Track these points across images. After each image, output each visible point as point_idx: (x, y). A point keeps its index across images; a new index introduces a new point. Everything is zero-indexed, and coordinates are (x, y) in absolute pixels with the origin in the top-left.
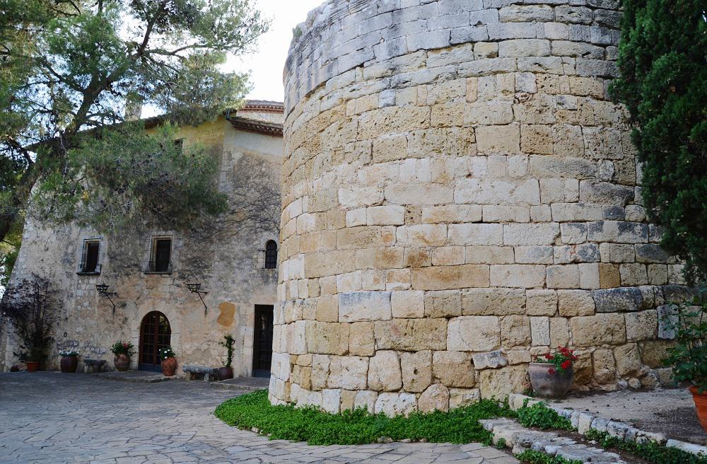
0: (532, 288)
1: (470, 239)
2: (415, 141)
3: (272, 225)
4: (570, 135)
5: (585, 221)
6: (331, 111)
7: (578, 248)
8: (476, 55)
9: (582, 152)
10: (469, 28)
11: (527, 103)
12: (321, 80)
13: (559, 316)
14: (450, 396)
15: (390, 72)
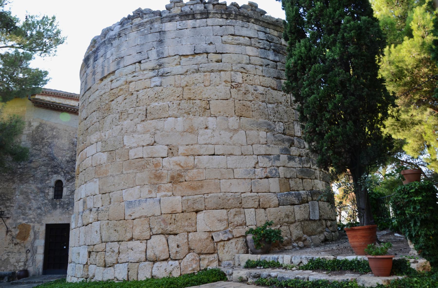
0: (245, 193)
1: (208, 165)
2: (174, 107)
3: (60, 170)
4: (261, 107)
5: (271, 155)
6: (118, 89)
7: (268, 170)
8: (209, 60)
9: (267, 117)
10: (205, 45)
11: (238, 88)
12: (112, 69)
13: (260, 208)
14: (200, 260)
15: (158, 67)
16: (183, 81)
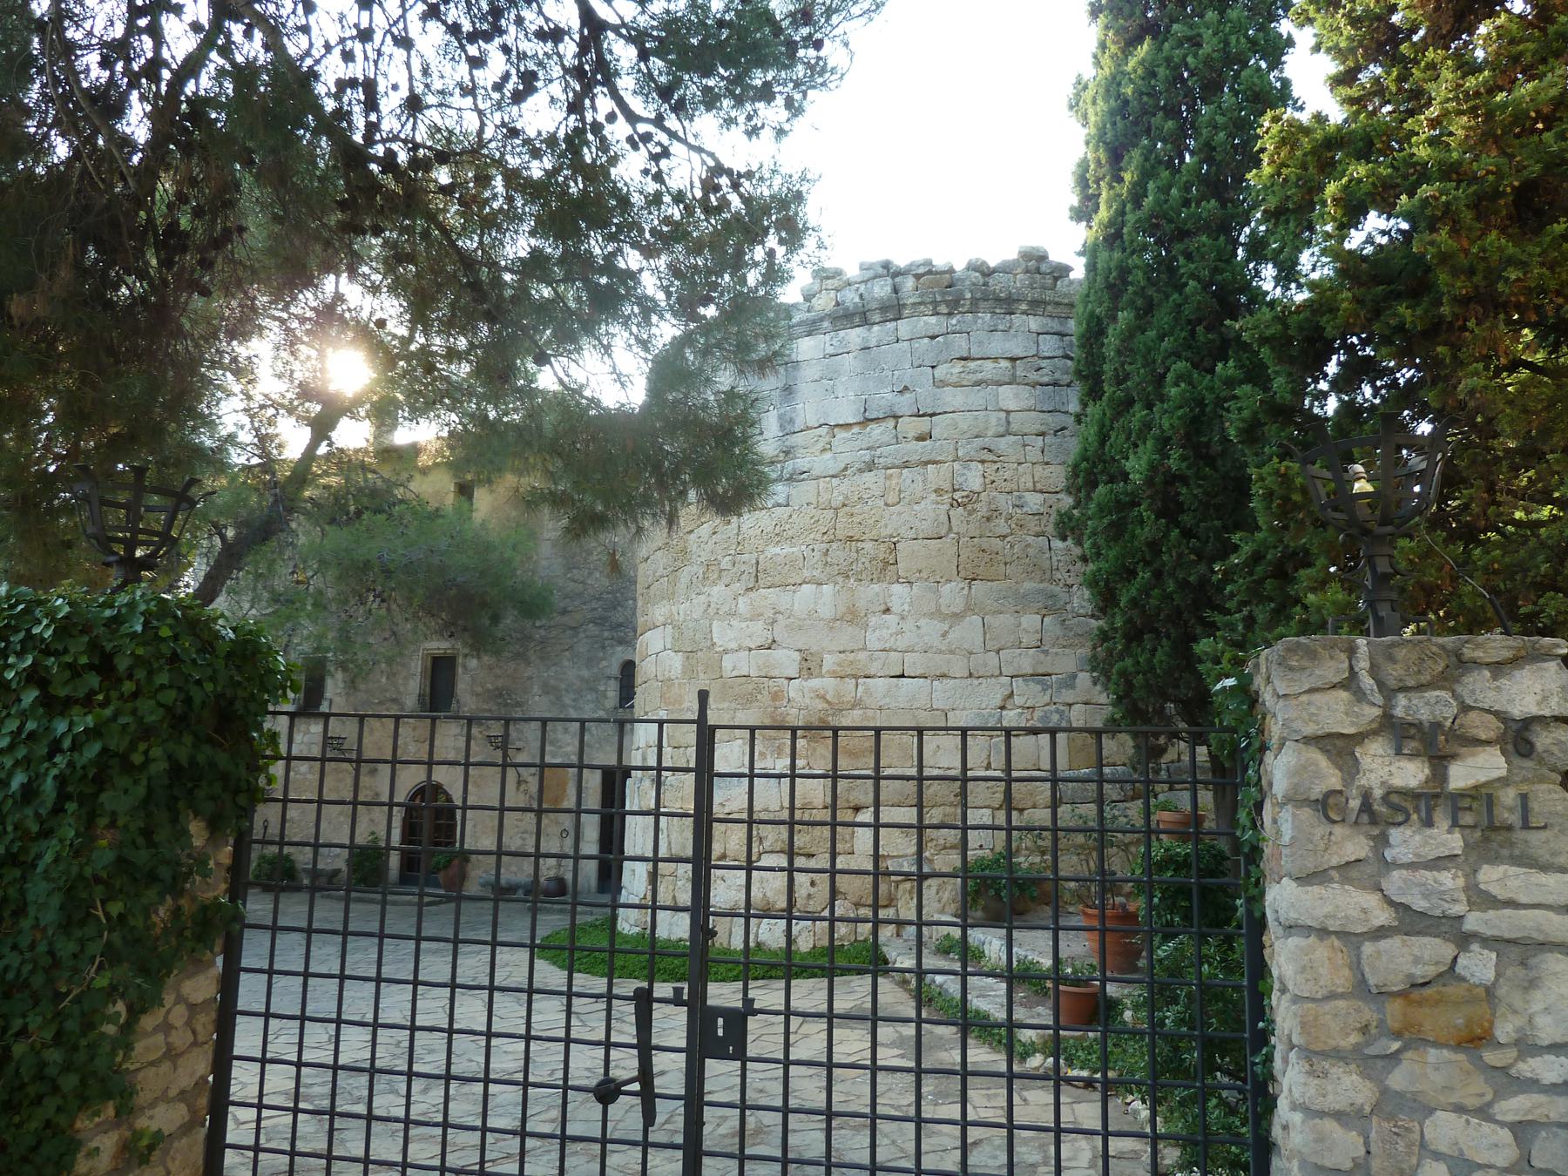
4: (1031, 551)
7: (1038, 714)
9: (1048, 576)
10: (890, 396)
11: (969, 507)
16: (836, 493)
